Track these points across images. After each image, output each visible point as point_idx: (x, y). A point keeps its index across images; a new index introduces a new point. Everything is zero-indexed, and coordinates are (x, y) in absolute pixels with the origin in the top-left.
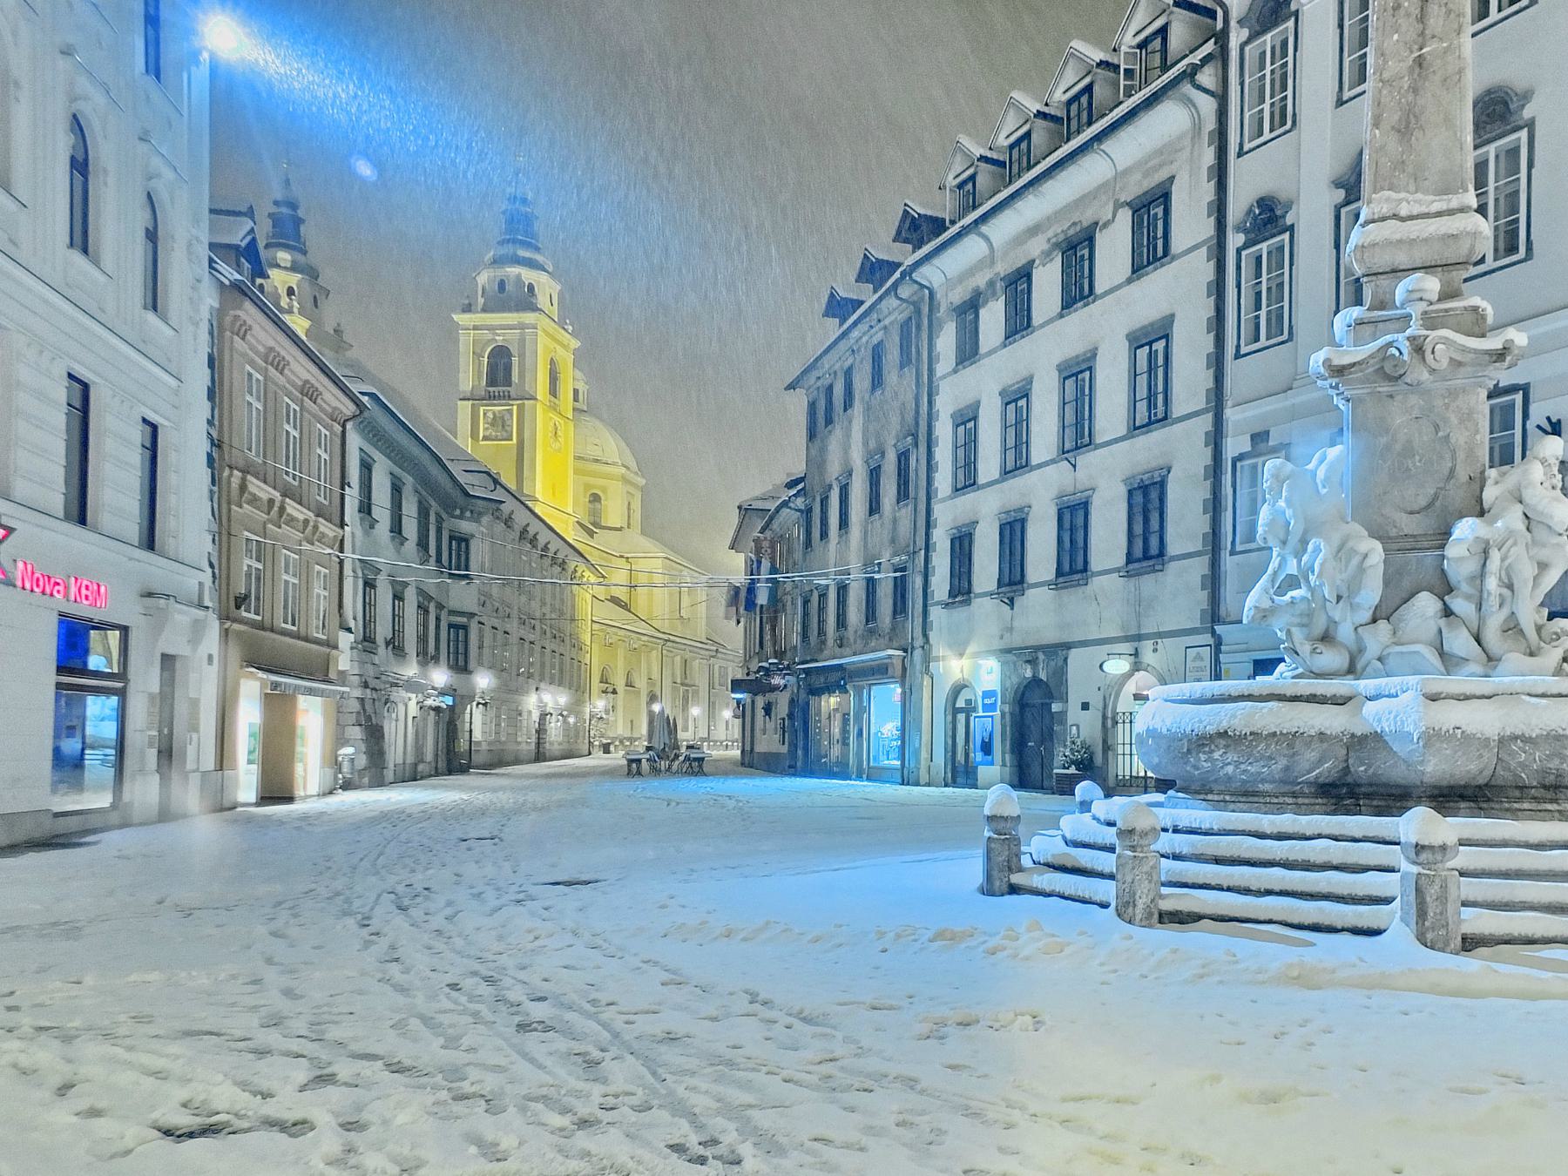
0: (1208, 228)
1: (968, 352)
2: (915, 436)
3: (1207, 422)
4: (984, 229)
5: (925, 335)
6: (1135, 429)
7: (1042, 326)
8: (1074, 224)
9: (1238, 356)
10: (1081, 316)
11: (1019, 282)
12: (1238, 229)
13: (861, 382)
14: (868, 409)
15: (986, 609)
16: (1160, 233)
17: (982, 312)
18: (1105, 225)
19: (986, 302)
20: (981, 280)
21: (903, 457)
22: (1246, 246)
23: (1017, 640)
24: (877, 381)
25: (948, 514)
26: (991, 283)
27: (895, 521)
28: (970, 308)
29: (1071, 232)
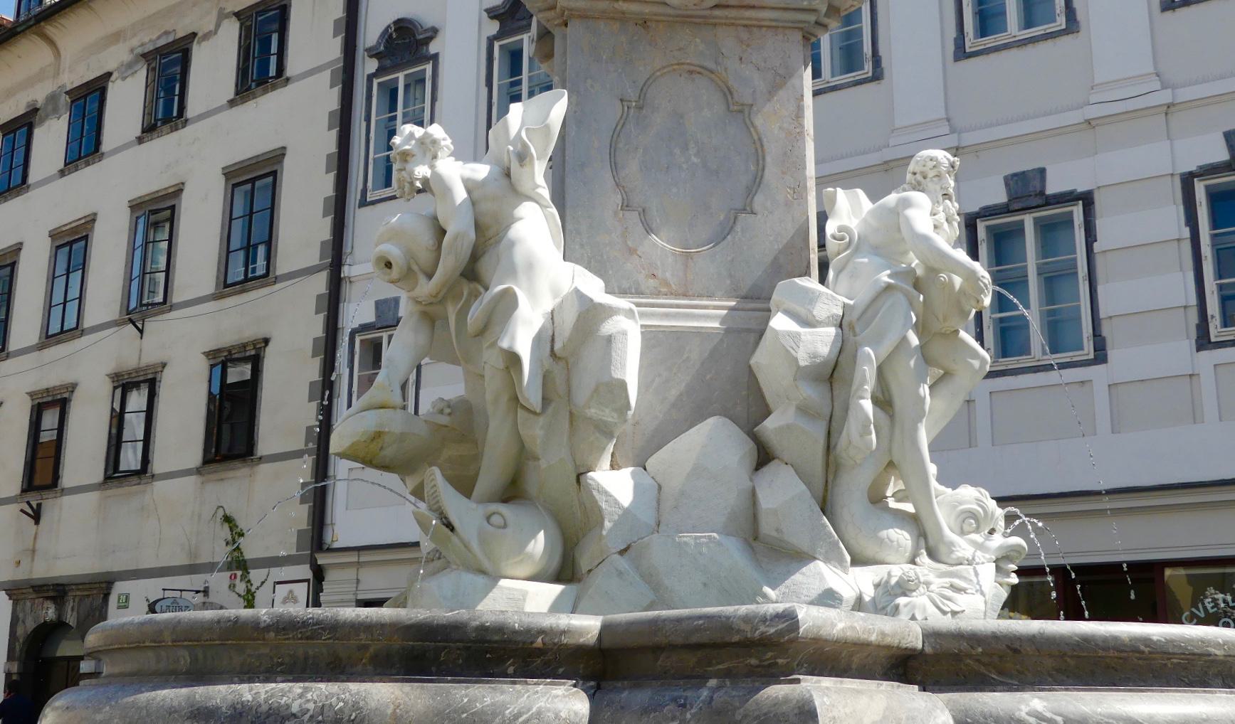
0: (333, 49)
3: (319, 284)
4: (50, 29)
6: (226, 287)
7: (116, 151)
8: (167, 33)
9: (364, 203)
10: (167, 144)
12: (373, 53)
16: (274, 49)
17: (37, 132)
18: (207, 36)
19: (42, 121)
20: (39, 94)
22: (380, 71)
23: (43, 570)
26: (52, 98)
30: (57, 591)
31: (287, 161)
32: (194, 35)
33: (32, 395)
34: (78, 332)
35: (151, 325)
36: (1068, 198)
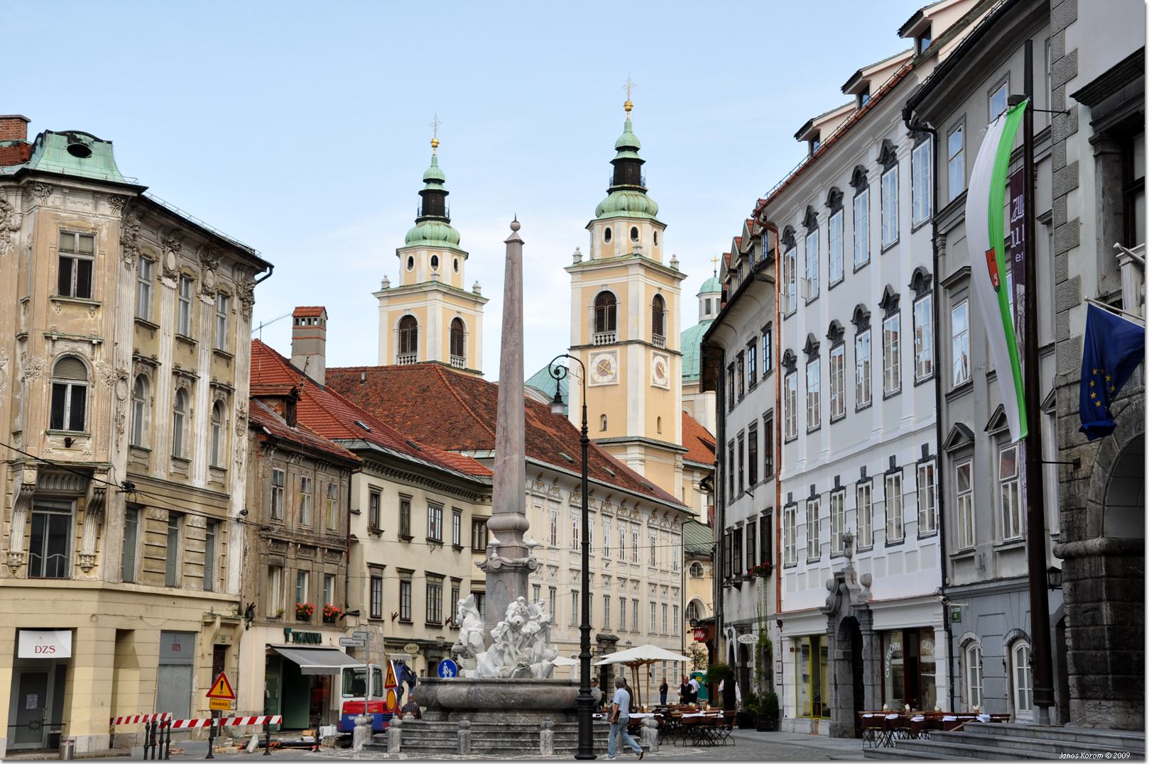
32: (755, 338)
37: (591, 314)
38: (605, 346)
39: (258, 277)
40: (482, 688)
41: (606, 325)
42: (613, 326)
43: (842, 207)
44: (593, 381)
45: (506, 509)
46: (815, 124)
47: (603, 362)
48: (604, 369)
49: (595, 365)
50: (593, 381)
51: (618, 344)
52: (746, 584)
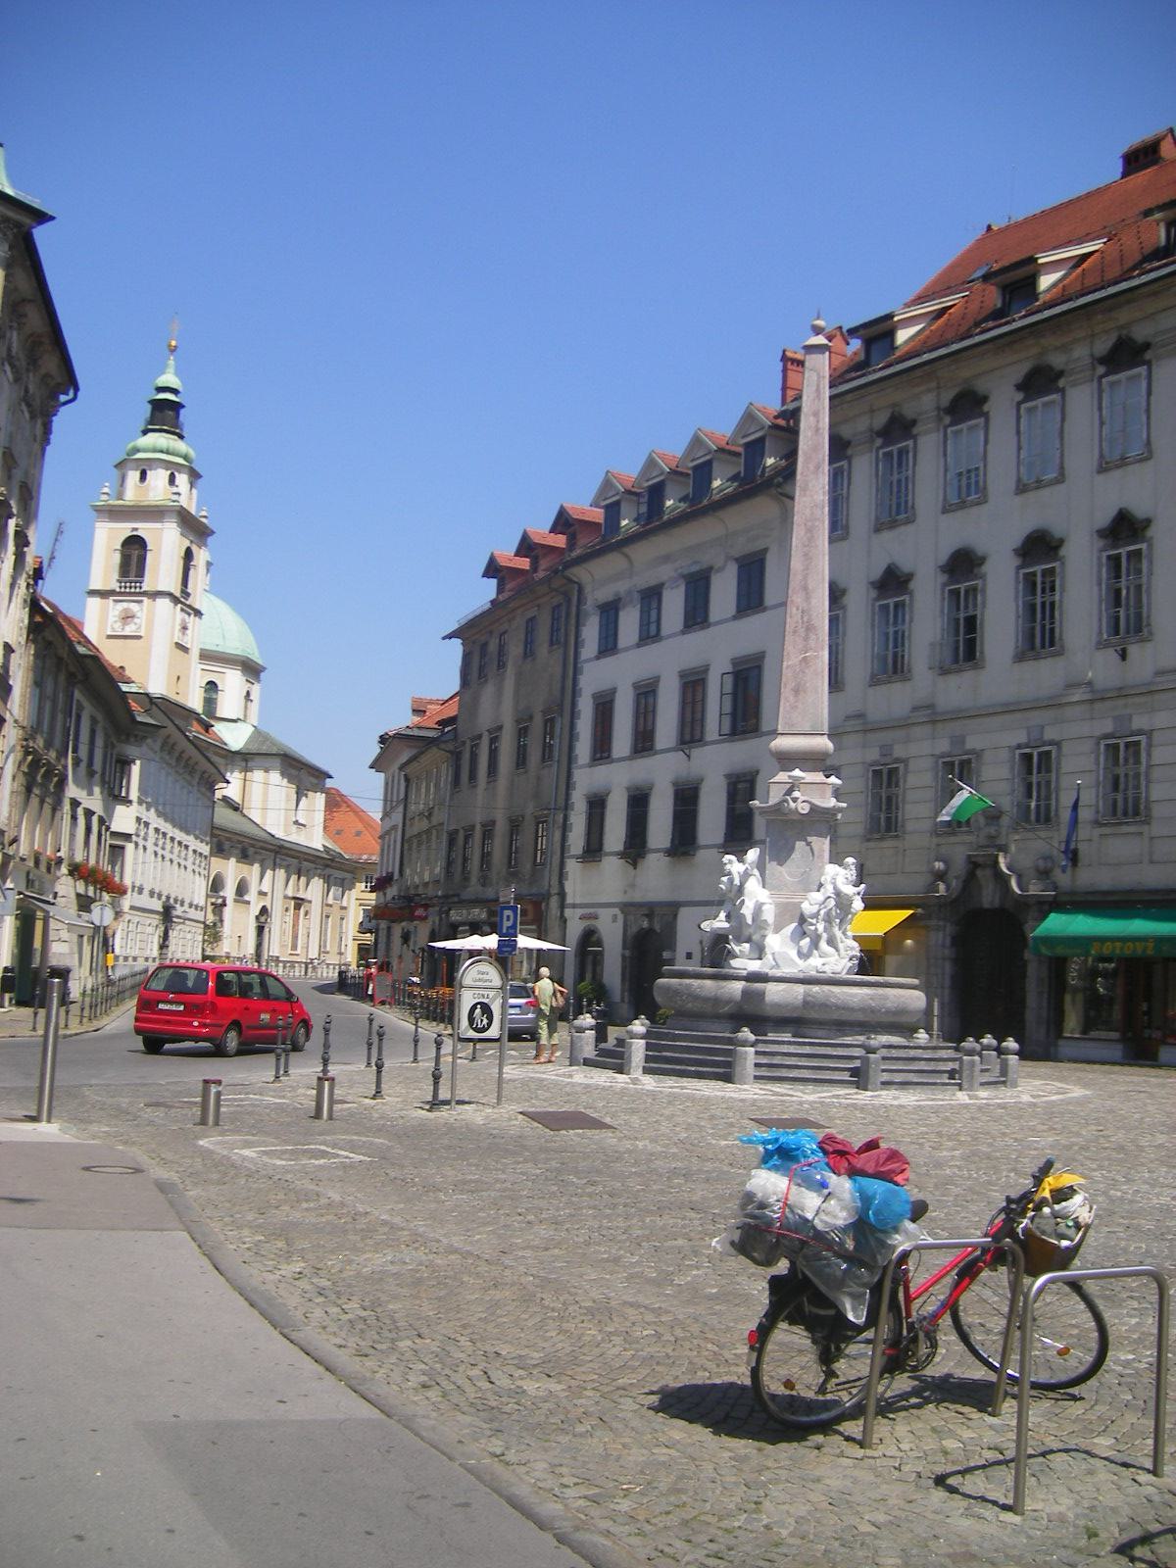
1: (609, 646)
2: (561, 706)
4: (626, 550)
5: (573, 621)
8: (695, 562)
10: (698, 638)
11: (651, 596)
13: (515, 649)
14: (519, 675)
15: (612, 867)
21: (549, 723)
23: (638, 897)
24: (529, 652)
25: (586, 779)
26: (629, 592)
27: (539, 778)
28: (610, 612)
29: (695, 568)
30: (650, 909)
31: (767, 660)
32: (710, 569)
33: (628, 789)
34: (651, 752)
35: (696, 752)
36: (1140, 732)
37: (117, 558)
38: (130, 594)
39: (63, 398)
40: (836, 989)
41: (133, 571)
42: (141, 573)
43: (986, 416)
44: (113, 629)
45: (807, 729)
46: (896, 319)
47: (126, 610)
48: (127, 617)
49: (117, 613)
50: (113, 629)
51: (145, 594)
52: (655, 864)
